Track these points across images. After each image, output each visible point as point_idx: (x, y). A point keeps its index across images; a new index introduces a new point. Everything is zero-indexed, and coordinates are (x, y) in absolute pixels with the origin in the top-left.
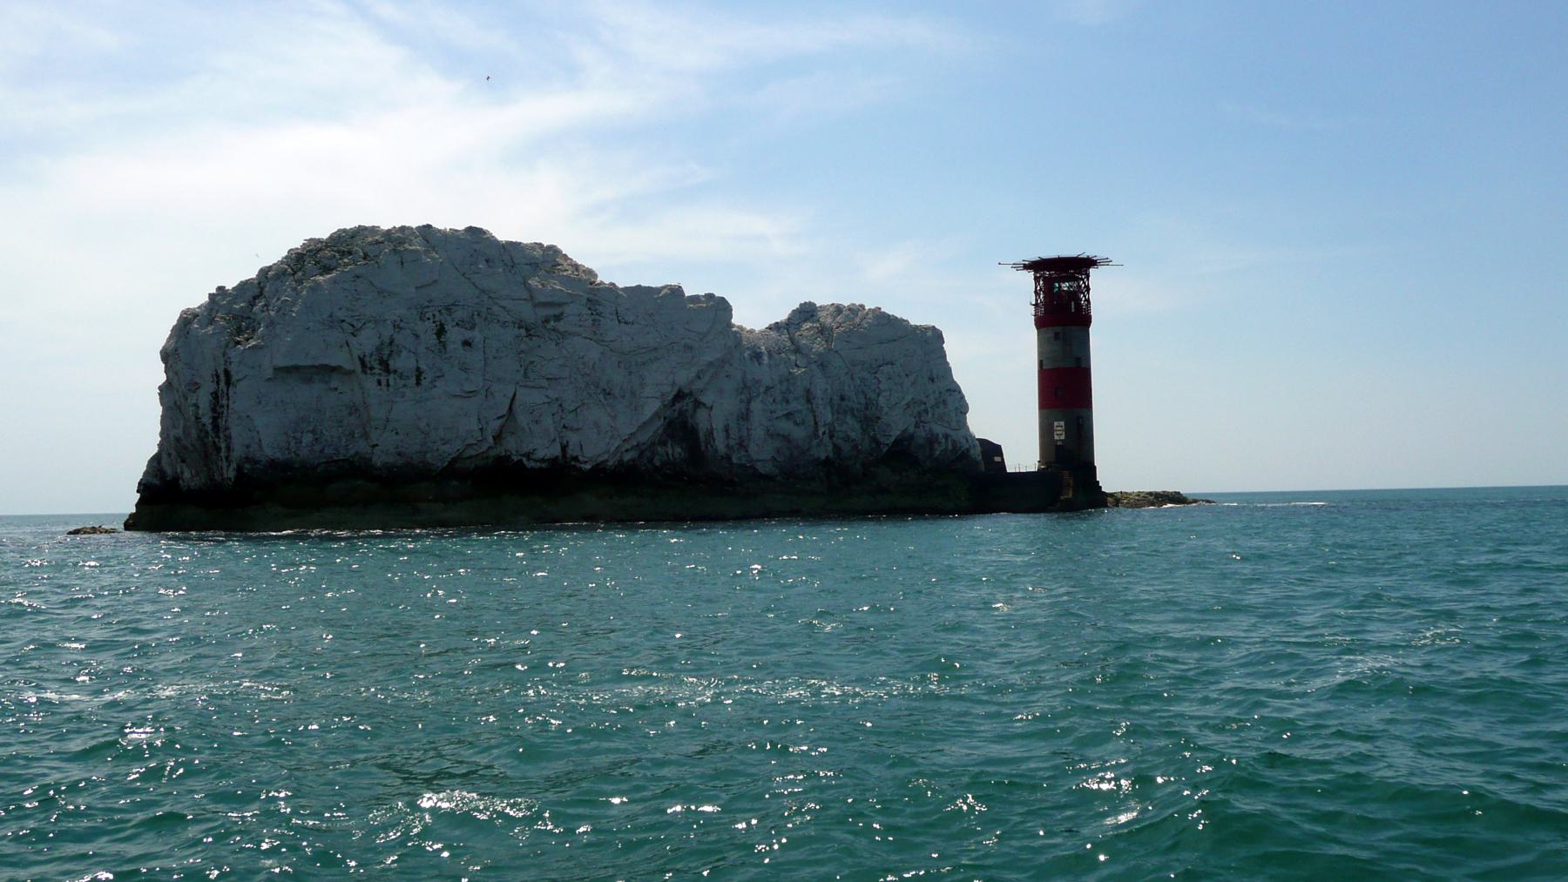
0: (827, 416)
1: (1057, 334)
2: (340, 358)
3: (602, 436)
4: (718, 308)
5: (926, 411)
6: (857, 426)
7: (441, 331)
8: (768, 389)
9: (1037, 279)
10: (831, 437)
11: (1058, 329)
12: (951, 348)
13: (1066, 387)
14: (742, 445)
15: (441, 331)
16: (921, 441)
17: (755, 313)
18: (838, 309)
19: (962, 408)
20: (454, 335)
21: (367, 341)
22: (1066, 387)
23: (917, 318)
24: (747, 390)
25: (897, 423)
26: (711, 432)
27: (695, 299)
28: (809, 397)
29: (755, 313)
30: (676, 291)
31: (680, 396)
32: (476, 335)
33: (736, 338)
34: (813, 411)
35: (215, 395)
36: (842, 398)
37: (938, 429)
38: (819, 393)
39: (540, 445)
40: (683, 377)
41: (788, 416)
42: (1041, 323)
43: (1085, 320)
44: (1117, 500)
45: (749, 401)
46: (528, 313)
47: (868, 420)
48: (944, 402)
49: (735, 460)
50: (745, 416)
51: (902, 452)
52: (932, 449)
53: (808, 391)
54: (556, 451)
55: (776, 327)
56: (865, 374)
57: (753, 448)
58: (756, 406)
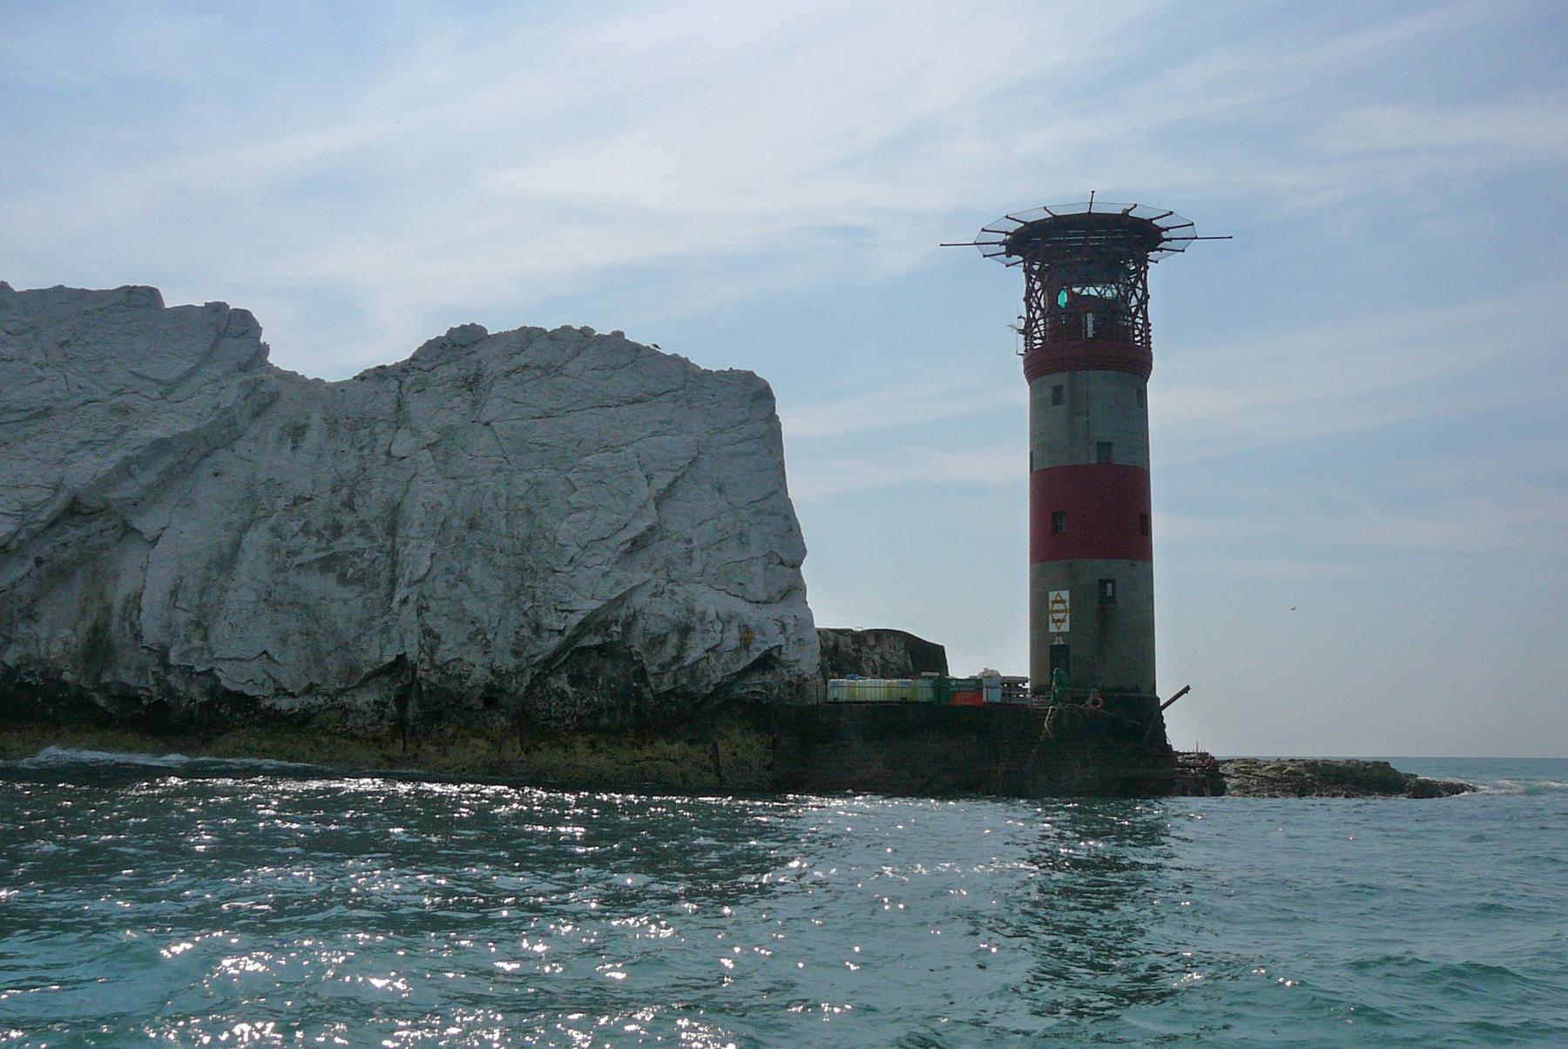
0: (418, 557)
1: (1057, 390)
5: (689, 557)
6: (495, 588)
8: (298, 500)
9: (1028, 272)
10: (422, 610)
11: (1061, 379)
12: (796, 422)
13: (1092, 515)
14: (201, 626)
16: (655, 627)
19: (787, 551)
22: (1092, 515)
26: (135, 600)
27: (185, 313)
28: (393, 519)
31: (75, 510)
33: (271, 397)
34: (393, 553)
36: (472, 526)
38: (415, 512)
40: (84, 472)
41: (327, 564)
42: (1036, 366)
43: (1138, 364)
44: (1206, 777)
45: (246, 527)
48: (742, 538)
49: (173, 659)
50: (226, 562)
51: (597, 649)
52: (682, 647)
53: (395, 509)
55: (381, 373)
56: (544, 474)
57: (221, 629)
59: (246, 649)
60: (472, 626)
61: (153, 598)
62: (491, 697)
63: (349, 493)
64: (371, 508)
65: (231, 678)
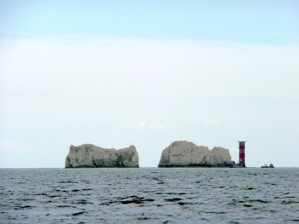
0: (218, 159)
2: (177, 154)
3: (198, 162)
4: (207, 148)
7: (185, 151)
13: (242, 156)
14: (210, 162)
15: (185, 151)
17: (211, 148)
18: (218, 147)
20: (186, 152)
21: (179, 153)
22: (242, 156)
23: (226, 148)
24: (210, 157)
25: (224, 160)
26: (207, 161)
28: (216, 157)
29: (211, 148)
30: (203, 146)
31: (205, 157)
32: (187, 152)
35: (168, 157)
37: (229, 160)
39: (194, 162)
40: (205, 155)
41: (214, 159)
46: (191, 149)
47: (222, 159)
50: (210, 159)
51: (225, 163)
54: (195, 162)
58: (211, 158)
59: (212, 163)
60: (220, 162)
61: (208, 161)
62: (221, 165)
63: (214, 155)
64: (215, 156)
65: (212, 164)
